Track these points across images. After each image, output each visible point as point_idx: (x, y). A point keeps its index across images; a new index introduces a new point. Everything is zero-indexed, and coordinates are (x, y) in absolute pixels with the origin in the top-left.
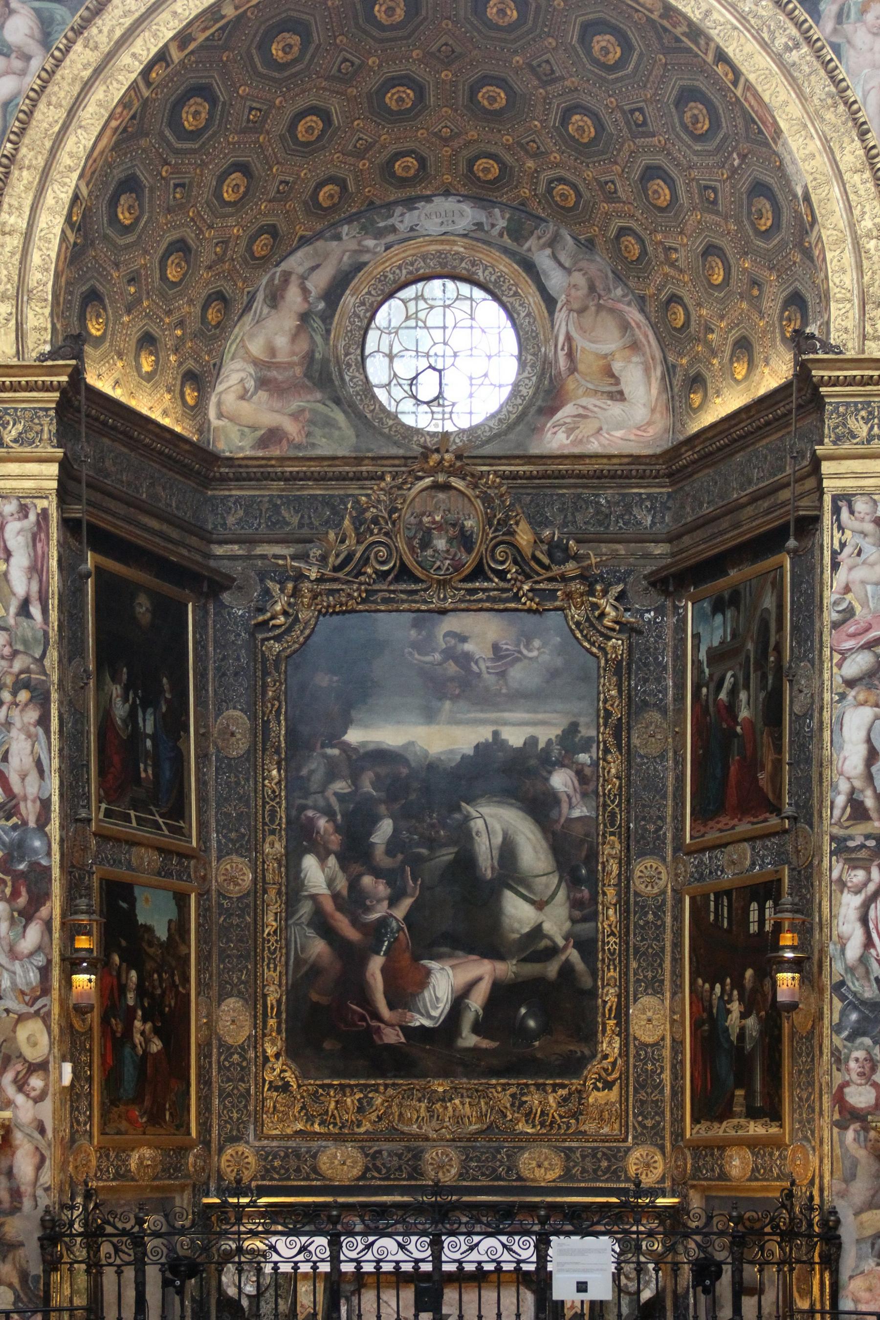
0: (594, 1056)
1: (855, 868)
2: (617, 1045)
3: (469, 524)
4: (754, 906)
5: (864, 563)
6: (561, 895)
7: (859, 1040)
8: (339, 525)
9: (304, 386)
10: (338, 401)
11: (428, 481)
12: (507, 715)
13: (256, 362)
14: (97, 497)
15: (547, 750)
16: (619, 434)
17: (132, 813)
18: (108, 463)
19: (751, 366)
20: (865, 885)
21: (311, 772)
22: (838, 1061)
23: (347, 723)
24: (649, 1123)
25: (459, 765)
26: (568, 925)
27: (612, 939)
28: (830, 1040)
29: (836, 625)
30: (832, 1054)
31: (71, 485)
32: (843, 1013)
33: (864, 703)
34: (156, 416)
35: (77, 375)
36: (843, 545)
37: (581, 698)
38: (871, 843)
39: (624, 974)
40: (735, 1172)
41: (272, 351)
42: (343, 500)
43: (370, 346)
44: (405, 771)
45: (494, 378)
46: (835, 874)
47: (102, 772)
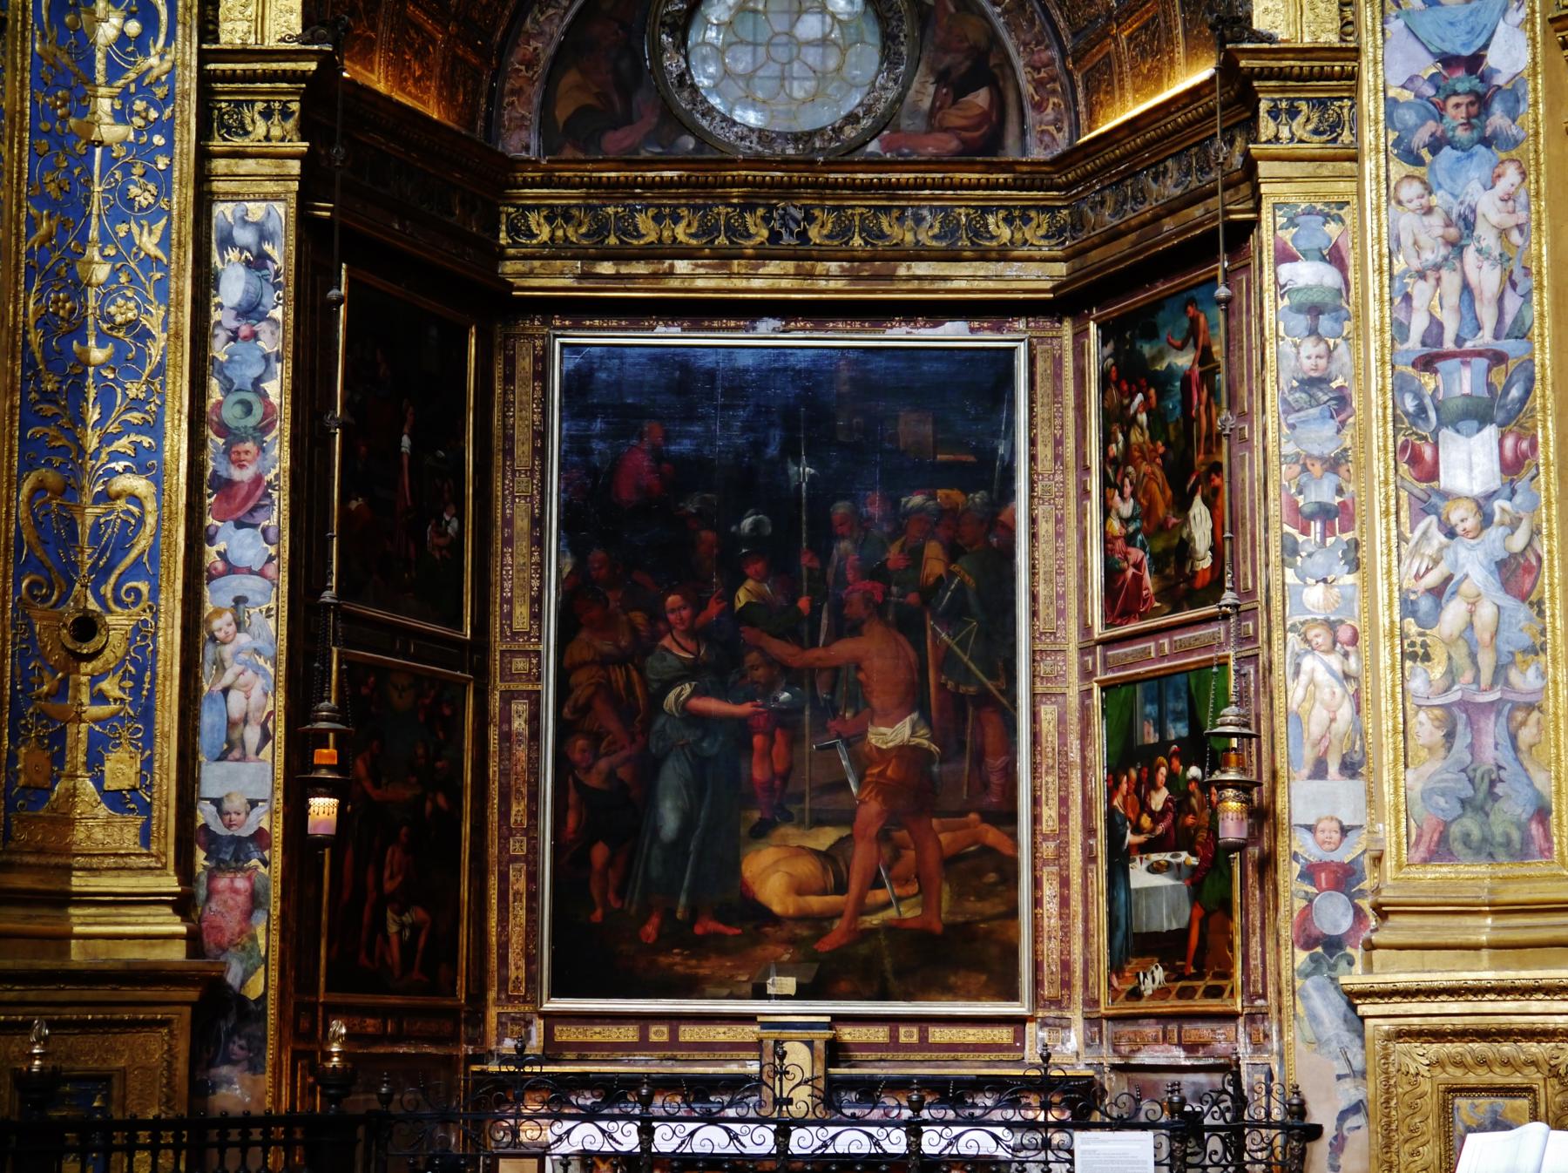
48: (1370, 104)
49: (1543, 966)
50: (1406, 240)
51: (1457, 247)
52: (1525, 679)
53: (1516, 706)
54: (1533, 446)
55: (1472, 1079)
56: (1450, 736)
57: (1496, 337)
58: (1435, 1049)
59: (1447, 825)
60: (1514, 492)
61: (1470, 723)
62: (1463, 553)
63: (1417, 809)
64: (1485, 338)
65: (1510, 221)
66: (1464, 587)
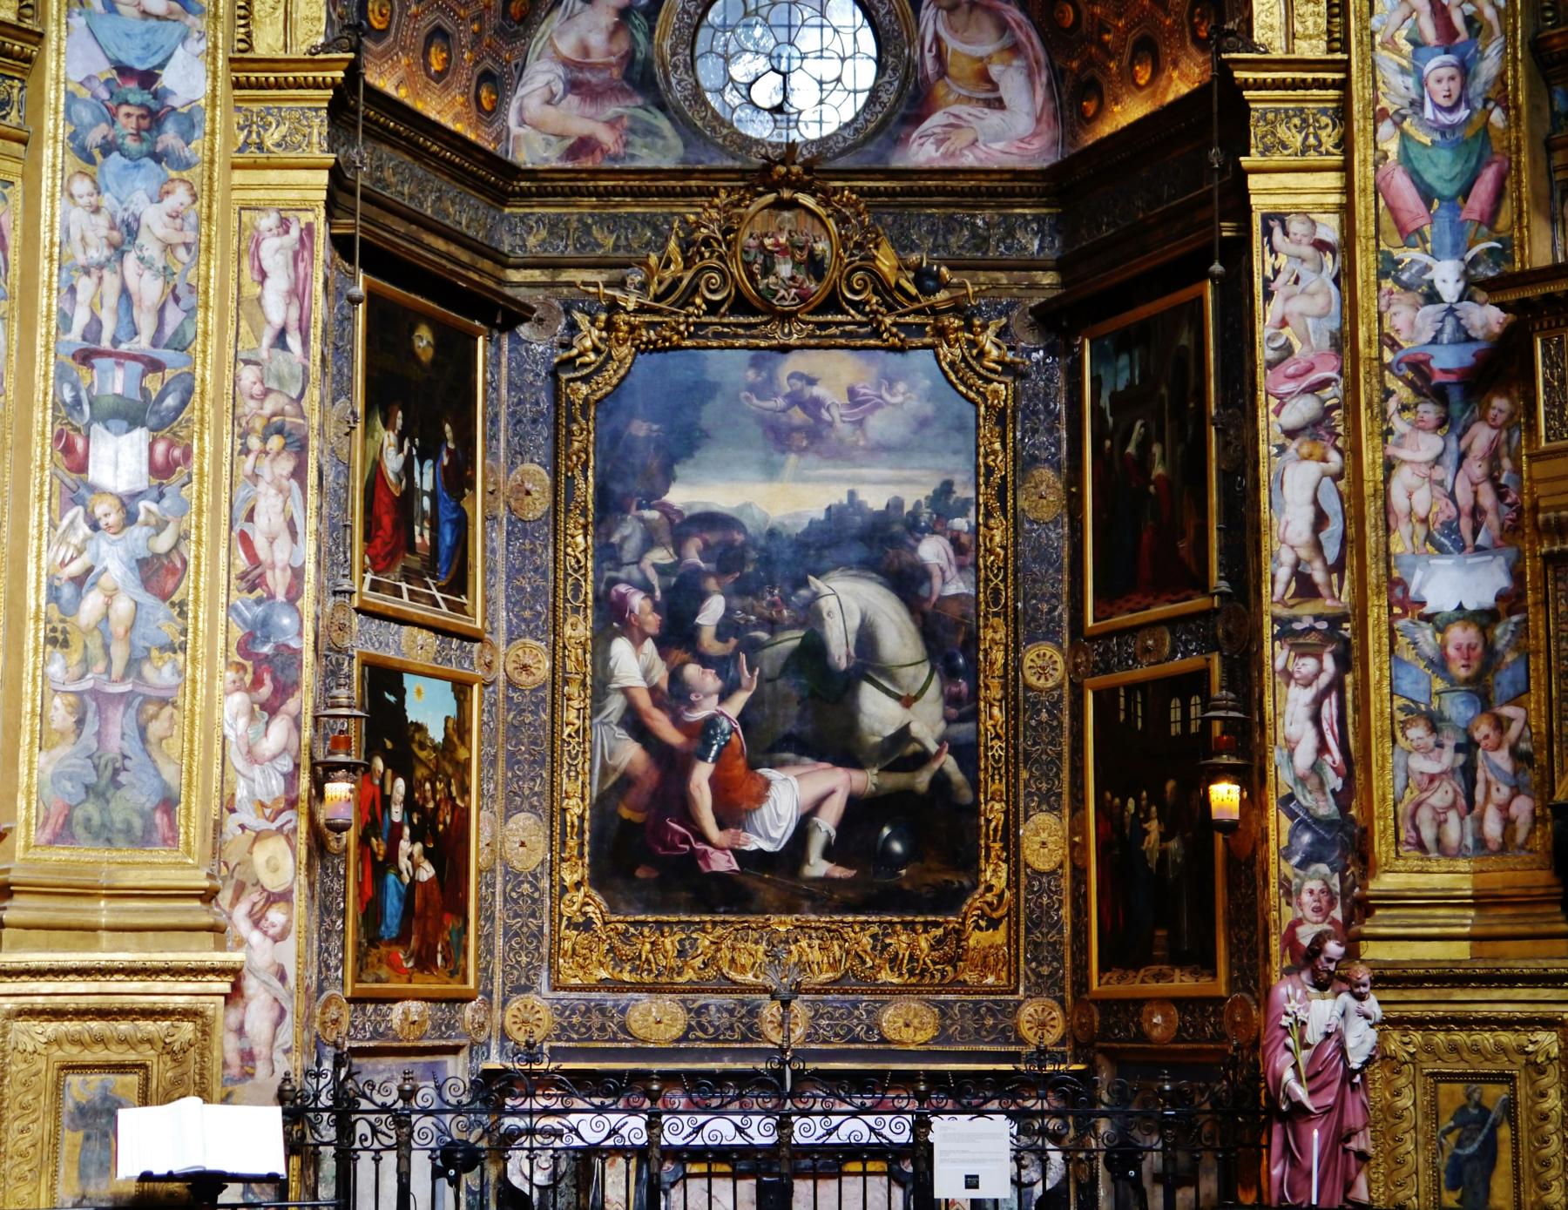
0: (975, 887)
1: (1303, 655)
2: (1004, 875)
3: (821, 247)
4: (1176, 703)
5: (1303, 292)
6: (934, 689)
7: (1314, 868)
8: (664, 246)
9: (622, 90)
10: (662, 107)
11: (770, 197)
12: (865, 472)
13: (566, 63)
14: (374, 211)
15: (914, 515)
16: (999, 146)
17: (404, 586)
18: (388, 174)
19: (1157, 72)
20: (1316, 676)
21: (624, 539)
22: (1288, 893)
23: (669, 478)
24: (1045, 970)
25: (807, 533)
26: (942, 726)
27: (997, 743)
28: (1279, 868)
29: (1271, 365)
30: (1281, 886)
31: (342, 197)
32: (1293, 834)
33: (1309, 457)
34: (447, 121)
35: (354, 70)
37: (956, 452)
38: (1323, 625)
39: (1012, 786)
40: (1156, 1033)
41: (585, 50)
42: (667, 219)
43: (701, 47)
44: (739, 538)
45: (848, 82)
46: (1279, 664)
47: (368, 536)
48: (53, 95)
49: (49, 947)
50: (75, 234)
51: (119, 250)
52: (160, 674)
53: (147, 700)
54: (187, 455)
55: (88, 1057)
56: (80, 722)
57: (155, 343)
58: (52, 1028)
59: (71, 809)
60: (162, 496)
61: (100, 711)
62: (104, 547)
63: (47, 791)
64: (142, 343)
65: (176, 238)
66: (103, 580)
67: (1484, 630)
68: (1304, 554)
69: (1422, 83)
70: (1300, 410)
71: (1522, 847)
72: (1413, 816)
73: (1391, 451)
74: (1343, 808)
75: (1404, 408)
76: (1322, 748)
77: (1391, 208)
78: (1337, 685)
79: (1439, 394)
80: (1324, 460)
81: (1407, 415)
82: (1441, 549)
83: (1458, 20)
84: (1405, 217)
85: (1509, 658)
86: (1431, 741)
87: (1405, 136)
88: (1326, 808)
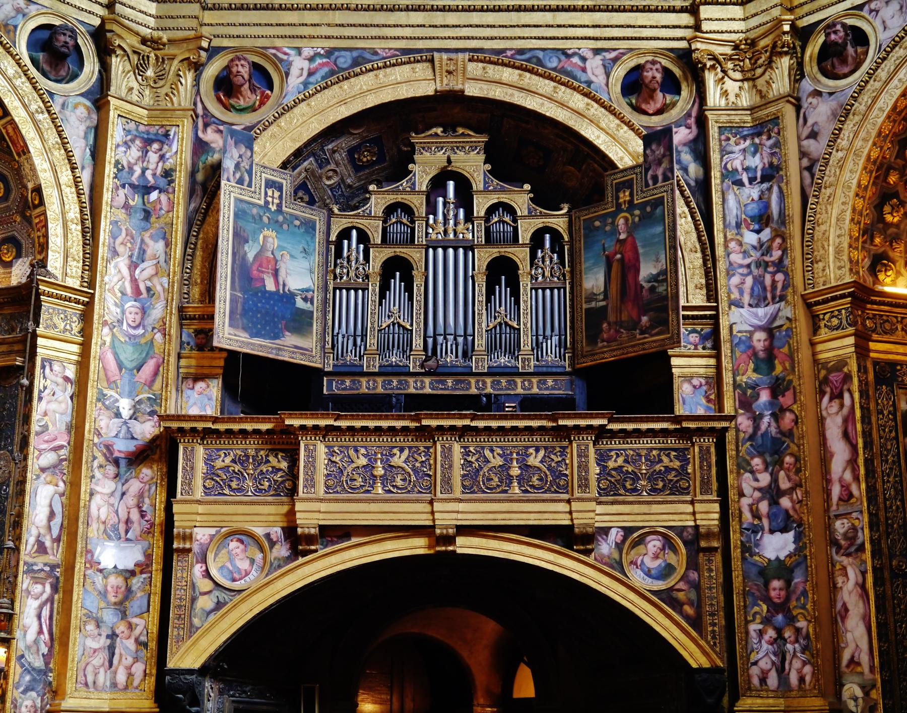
1: (37, 583)
5: (56, 400)
20: (41, 594)
29: (38, 434)
30: (12, 703)
32: (21, 676)
36: (45, 388)
46: (25, 586)
67: (126, 579)
68: (42, 531)
69: (123, 312)
70: (48, 459)
71: (137, 688)
72: (85, 670)
73: (93, 486)
74: (47, 664)
75: (101, 466)
76: (40, 632)
77: (104, 369)
78: (51, 600)
79: (116, 462)
80: (57, 485)
81: (101, 470)
82: (110, 538)
83: (142, 287)
84: (110, 374)
85: (139, 594)
86: (96, 632)
87: (113, 335)
88: (39, 663)
